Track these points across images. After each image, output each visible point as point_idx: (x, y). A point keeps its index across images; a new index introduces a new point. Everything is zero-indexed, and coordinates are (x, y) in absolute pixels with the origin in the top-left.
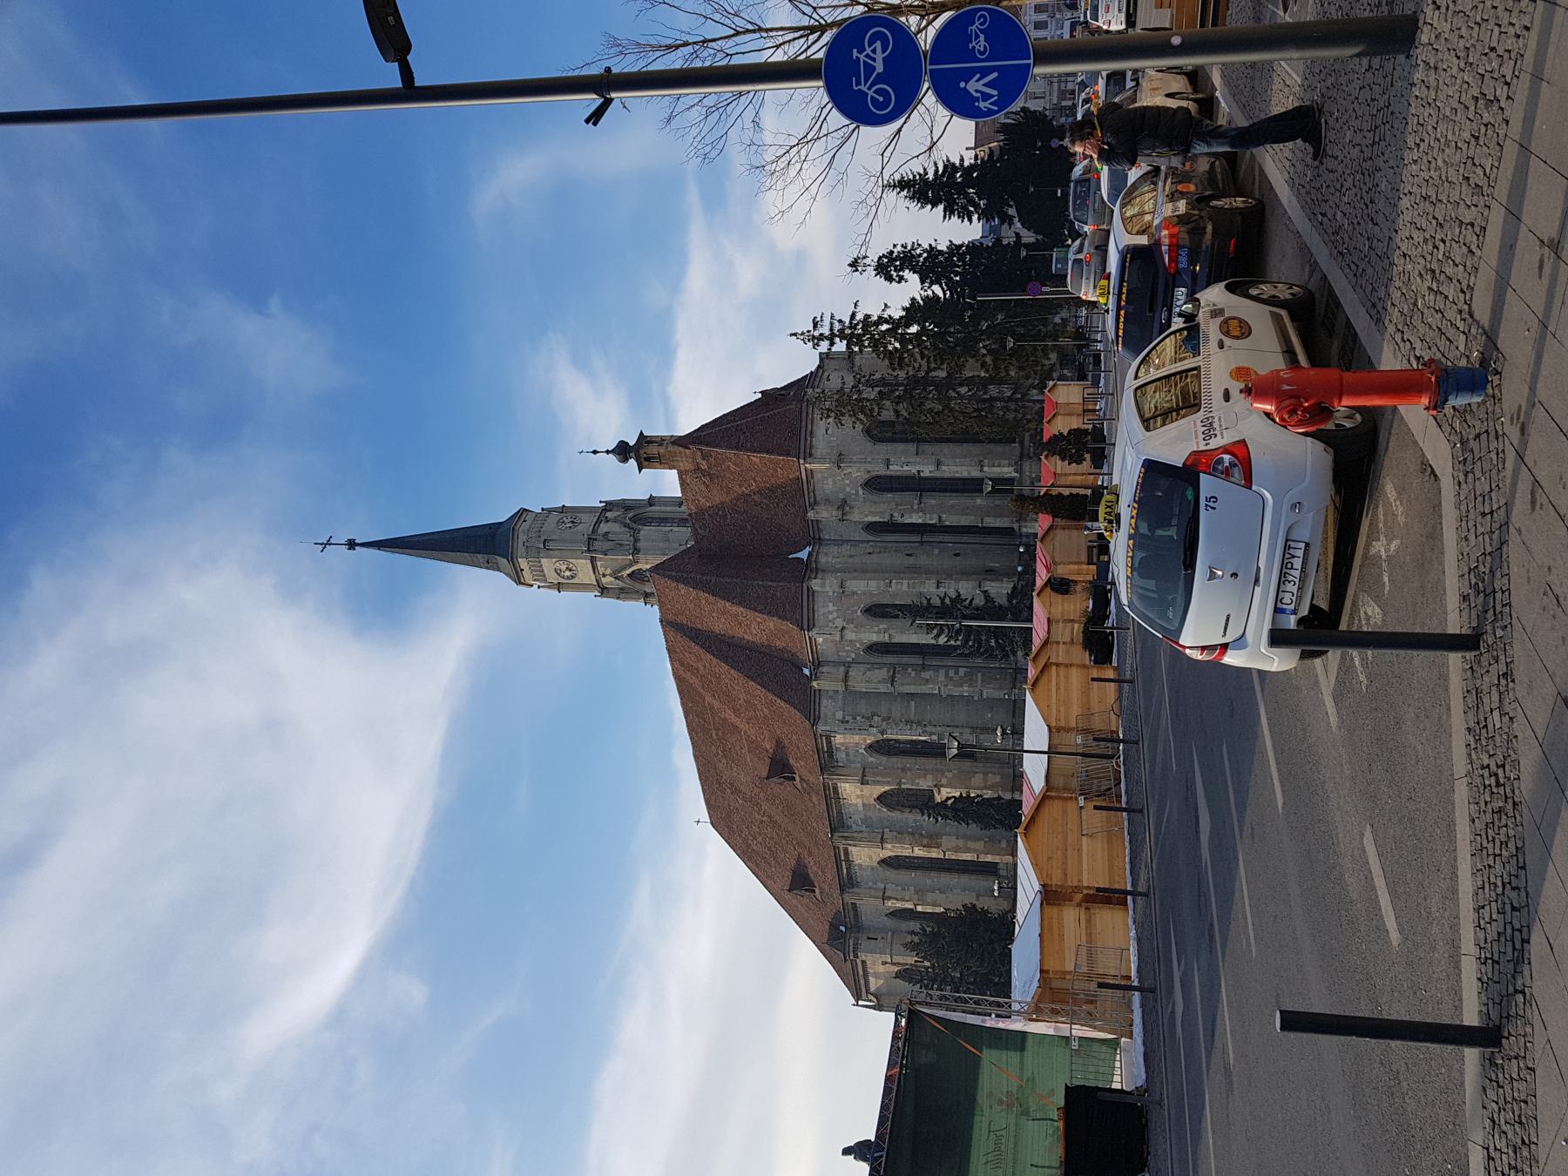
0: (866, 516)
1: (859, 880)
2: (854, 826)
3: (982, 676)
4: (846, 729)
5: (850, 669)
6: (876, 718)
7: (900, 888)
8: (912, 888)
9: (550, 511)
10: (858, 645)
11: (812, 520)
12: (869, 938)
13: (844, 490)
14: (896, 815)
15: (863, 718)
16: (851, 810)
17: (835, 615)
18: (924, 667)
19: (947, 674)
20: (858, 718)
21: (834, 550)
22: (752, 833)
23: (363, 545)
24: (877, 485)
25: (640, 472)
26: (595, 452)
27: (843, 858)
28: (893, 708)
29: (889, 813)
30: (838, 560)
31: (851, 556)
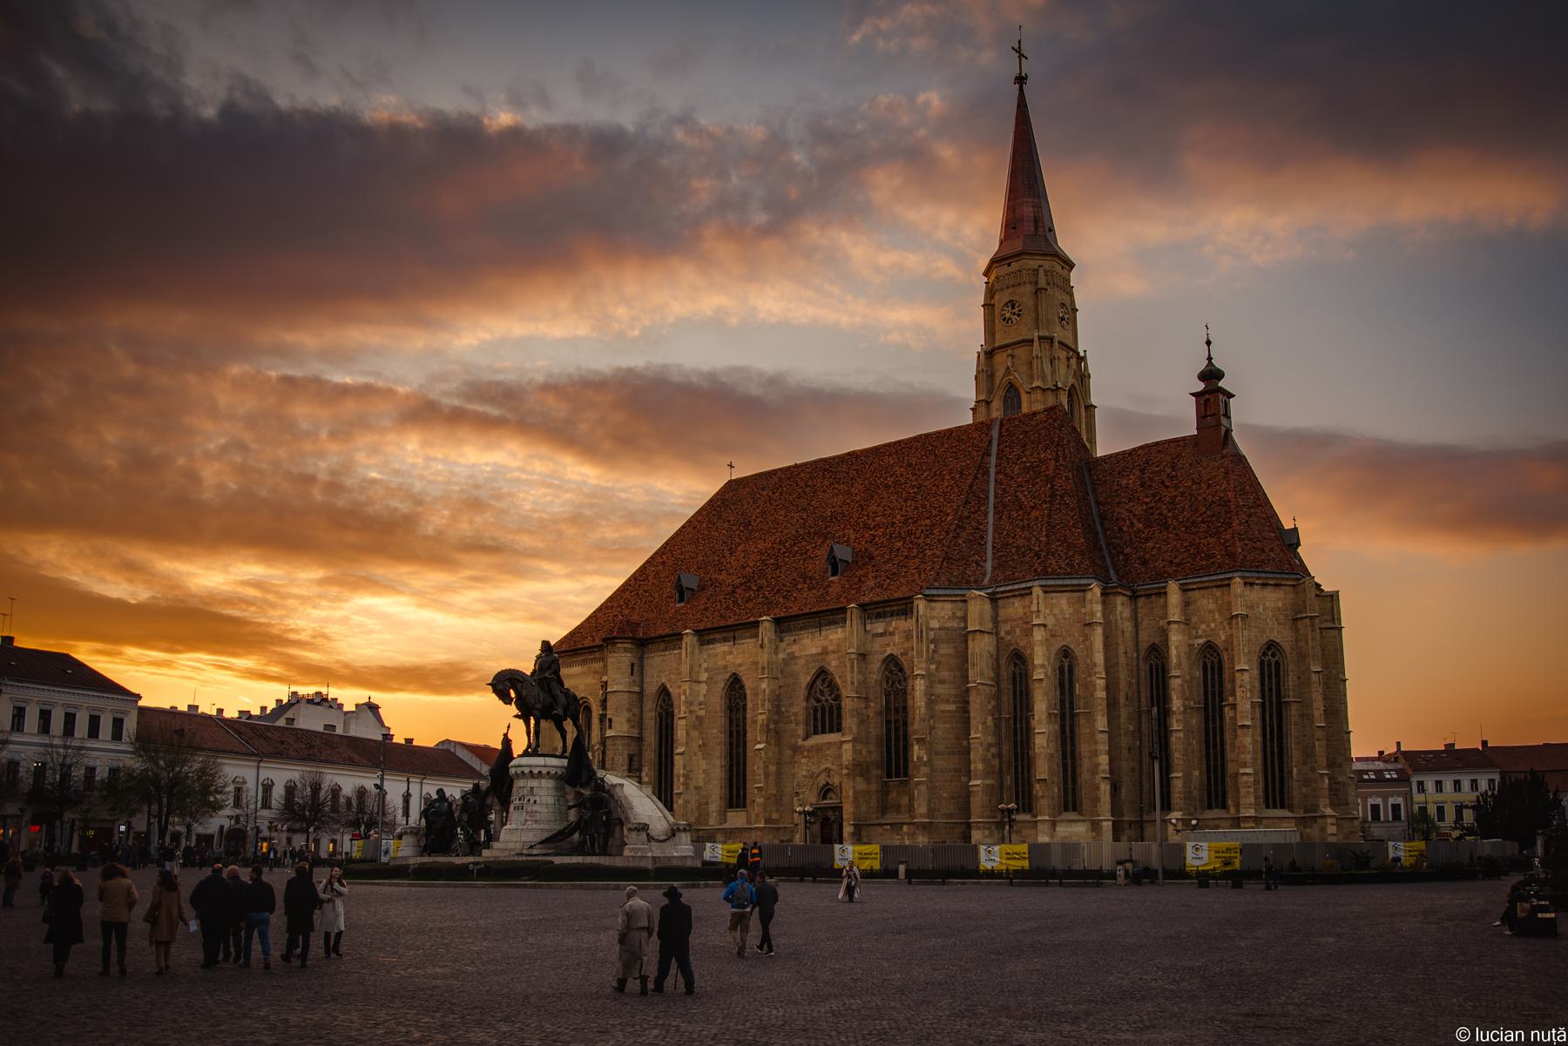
0: (1177, 648)
3: (992, 785)
5: (990, 635)
6: (933, 667)
7: (702, 699)
8: (702, 713)
9: (1071, 295)
11: (1165, 587)
12: (633, 665)
13: (1203, 622)
14: (802, 693)
15: (934, 651)
19: (990, 745)
20: (932, 646)
21: (1127, 613)
23: (1021, 89)
25: (1191, 394)
28: (946, 686)
30: (1119, 618)
31: (1123, 632)
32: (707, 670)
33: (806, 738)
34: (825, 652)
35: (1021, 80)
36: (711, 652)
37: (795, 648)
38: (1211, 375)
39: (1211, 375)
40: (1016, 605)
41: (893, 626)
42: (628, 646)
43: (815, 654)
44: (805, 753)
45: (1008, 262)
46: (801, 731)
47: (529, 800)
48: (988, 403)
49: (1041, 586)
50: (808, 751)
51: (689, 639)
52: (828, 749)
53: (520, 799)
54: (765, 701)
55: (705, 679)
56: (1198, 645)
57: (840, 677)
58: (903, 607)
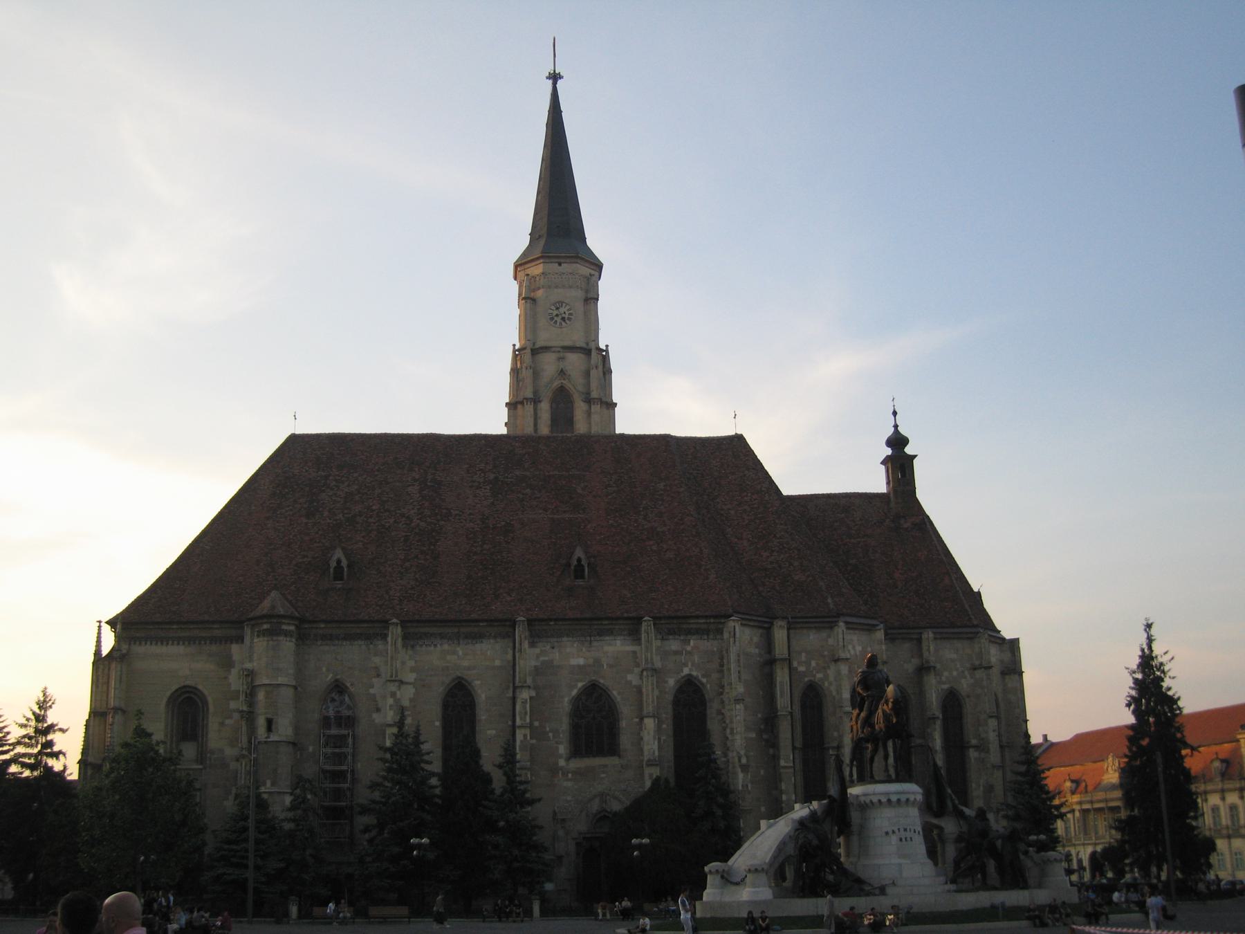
1: (418, 648)
2: (537, 651)
4: (739, 656)
10: (819, 676)
11: (921, 633)
14: (565, 705)
16: (568, 650)
17: (852, 652)
18: (794, 748)
22: (357, 498)
24: (952, 702)
26: (895, 413)
29: (566, 699)
32: (413, 670)
33: (568, 759)
34: (597, 662)
35: (555, 77)
37: (556, 656)
38: (897, 442)
39: (897, 442)
40: (811, 637)
42: (292, 628)
44: (570, 775)
45: (559, 260)
46: (562, 749)
47: (915, 832)
48: (536, 401)
49: (846, 623)
51: (395, 632)
53: (905, 830)
54: (526, 713)
55: (412, 680)
56: (942, 689)
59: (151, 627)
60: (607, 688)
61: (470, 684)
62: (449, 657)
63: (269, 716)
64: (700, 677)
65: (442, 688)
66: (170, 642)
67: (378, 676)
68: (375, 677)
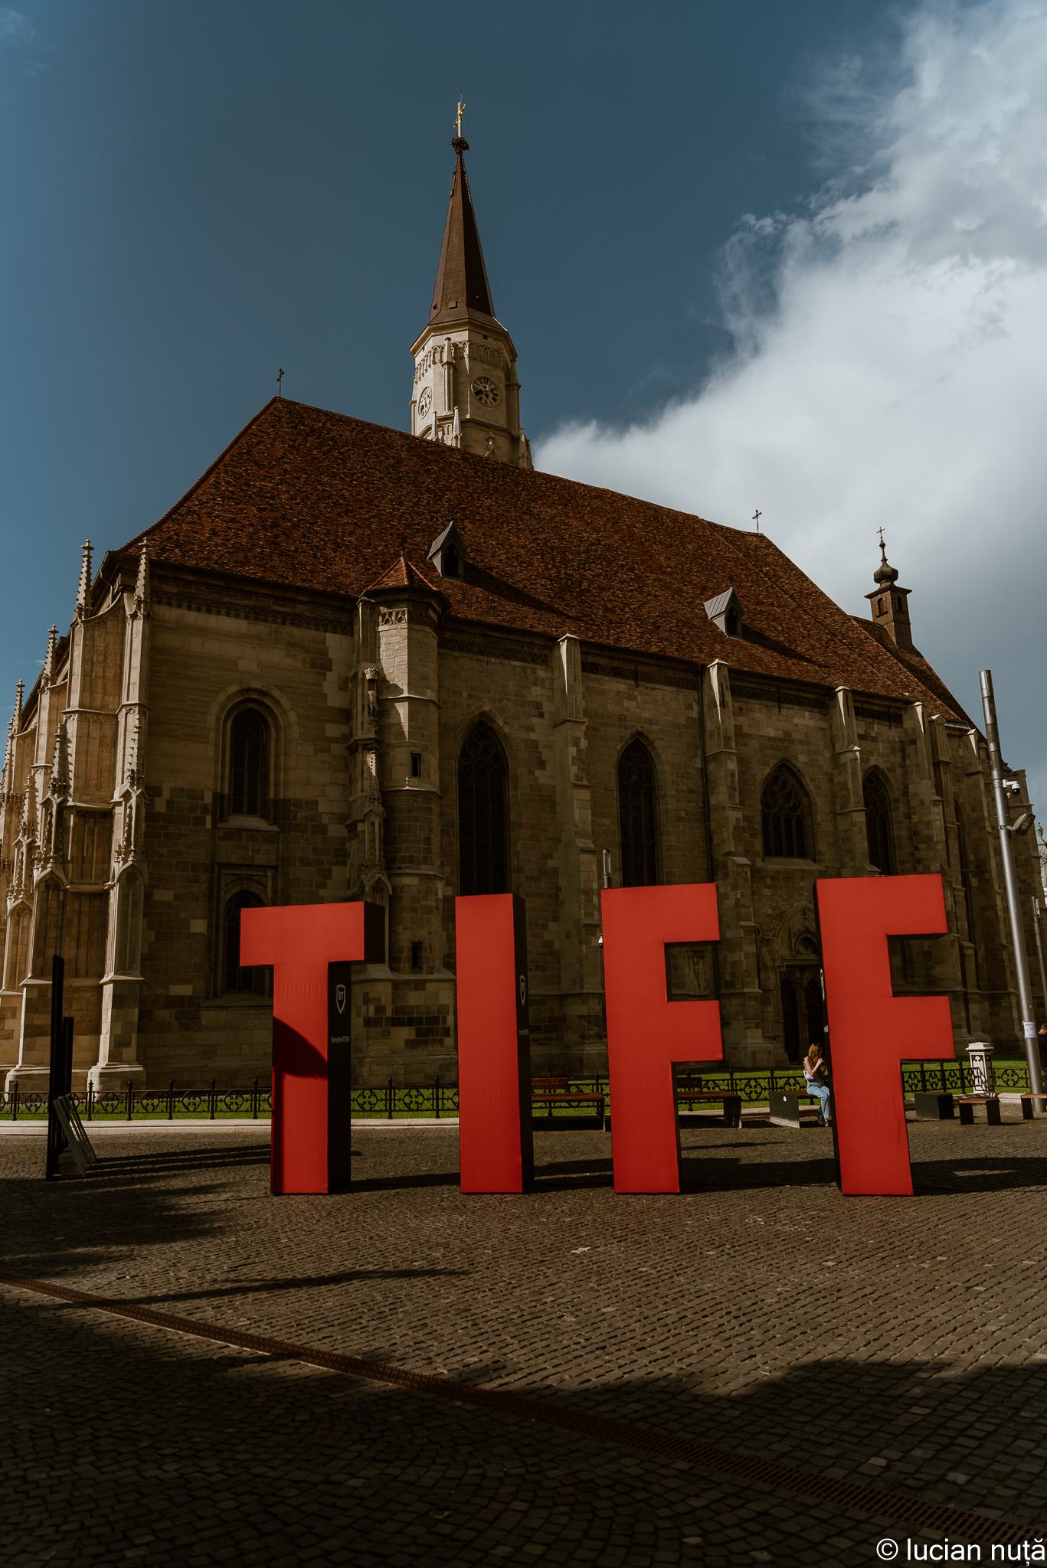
16: (757, 715)
23: (461, 159)
26: (883, 546)
27: (641, 668)
34: (787, 738)
36: (594, 685)
38: (887, 576)
39: (887, 576)
41: (876, 730)
43: (774, 739)
44: (768, 880)
45: (484, 333)
50: (773, 878)
52: (802, 879)
54: (734, 789)
57: (812, 780)
58: (886, 710)
59: (191, 578)
60: (799, 771)
61: (651, 743)
62: (626, 703)
63: (417, 750)
64: (886, 771)
65: (619, 746)
66: (224, 611)
67: (541, 715)
68: (535, 716)
